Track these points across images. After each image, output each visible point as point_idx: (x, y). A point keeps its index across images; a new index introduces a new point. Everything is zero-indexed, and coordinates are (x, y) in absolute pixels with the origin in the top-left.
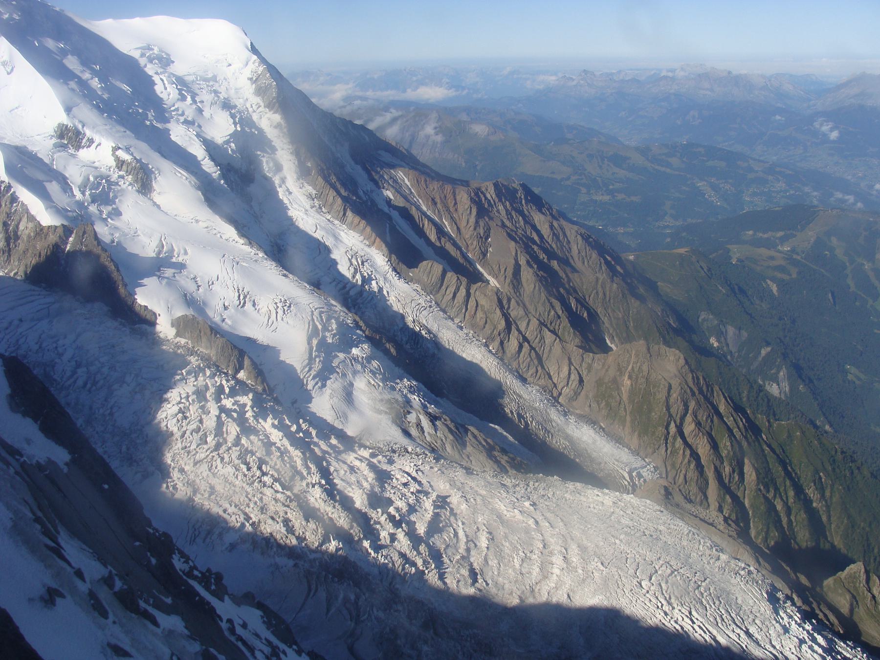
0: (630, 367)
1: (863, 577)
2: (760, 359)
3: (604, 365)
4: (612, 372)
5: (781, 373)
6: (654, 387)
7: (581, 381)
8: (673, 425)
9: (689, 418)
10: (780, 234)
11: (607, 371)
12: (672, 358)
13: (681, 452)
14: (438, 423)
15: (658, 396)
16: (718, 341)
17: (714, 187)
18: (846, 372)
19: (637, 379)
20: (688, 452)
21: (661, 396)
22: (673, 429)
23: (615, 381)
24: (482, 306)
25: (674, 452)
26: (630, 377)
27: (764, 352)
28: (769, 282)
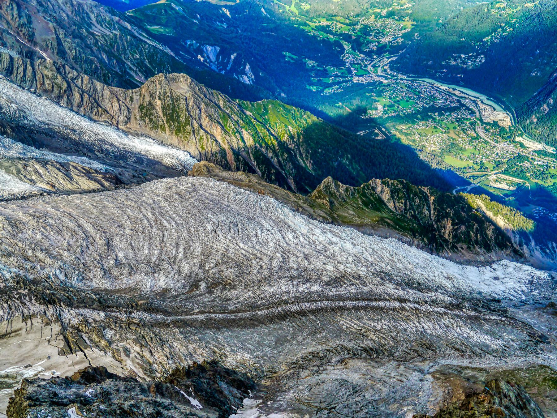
0: (158, 93)
1: (333, 185)
2: (231, 62)
3: (140, 96)
4: (147, 99)
6: (177, 101)
7: (128, 109)
8: (195, 122)
9: (204, 115)
11: (144, 98)
12: (182, 80)
13: (205, 138)
14: (49, 167)
16: (203, 57)
18: (285, 56)
19: (164, 99)
20: (209, 137)
22: (196, 125)
23: (150, 104)
24: (47, 76)
25: (201, 139)
26: (160, 99)
27: (233, 57)
28: (224, 9)
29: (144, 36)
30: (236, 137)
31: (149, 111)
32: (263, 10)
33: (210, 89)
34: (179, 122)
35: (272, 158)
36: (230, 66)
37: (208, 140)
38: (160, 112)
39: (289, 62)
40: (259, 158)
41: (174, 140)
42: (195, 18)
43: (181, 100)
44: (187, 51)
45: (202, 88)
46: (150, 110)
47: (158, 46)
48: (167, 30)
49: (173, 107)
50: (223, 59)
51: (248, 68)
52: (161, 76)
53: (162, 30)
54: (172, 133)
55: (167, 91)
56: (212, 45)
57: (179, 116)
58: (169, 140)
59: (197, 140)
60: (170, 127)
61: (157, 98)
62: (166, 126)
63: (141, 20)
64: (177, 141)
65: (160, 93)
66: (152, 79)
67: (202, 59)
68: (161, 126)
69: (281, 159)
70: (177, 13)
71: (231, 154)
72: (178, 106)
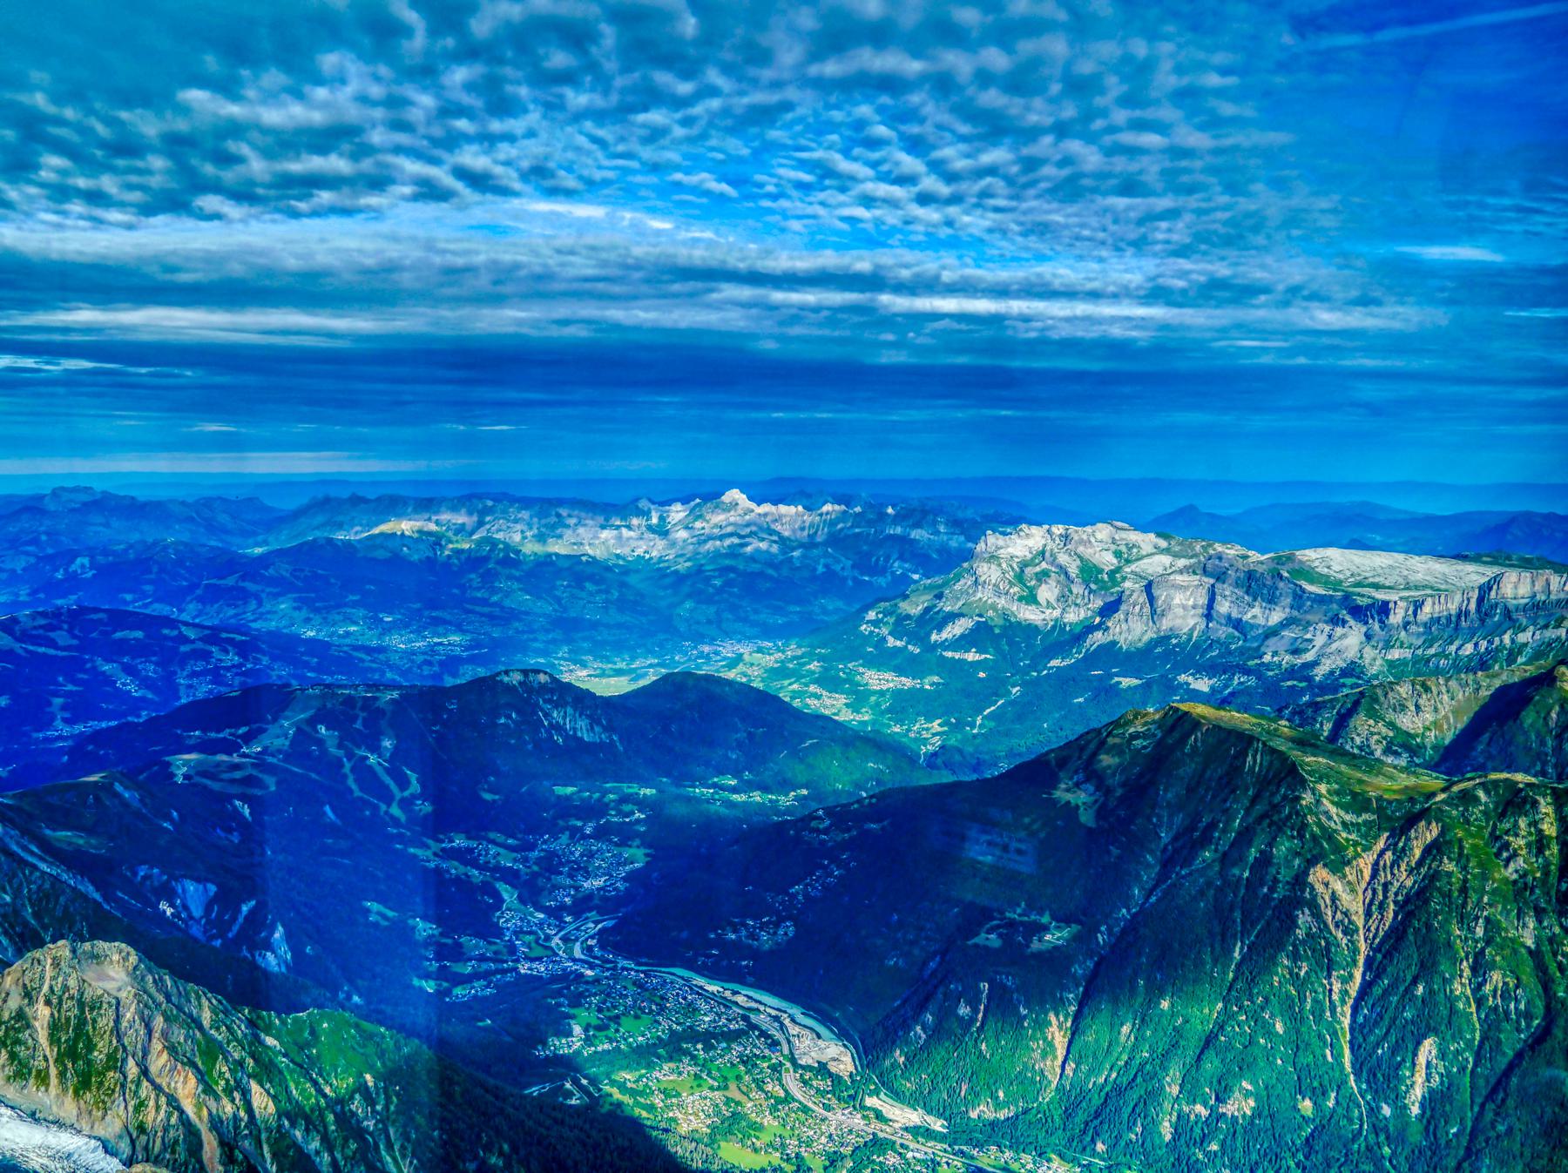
0: (46, 988)
2: (241, 919)
5: (277, 935)
6: (92, 1009)
8: (131, 1062)
9: (157, 1045)
10: (241, 731)
12: (116, 957)
13: (152, 1103)
15: (101, 1023)
16: (172, 905)
17: (129, 670)
18: (368, 911)
19: (60, 1003)
20: (163, 1100)
21: (105, 1022)
22: (132, 1069)
23: (20, 1015)
26: (48, 1003)
27: (245, 909)
28: (237, 803)
29: (32, 853)
30: (233, 1101)
31: (12, 1033)
32: (327, 809)
33: (180, 983)
34: (89, 1063)
35: (317, 1153)
36: (236, 928)
37: (158, 1108)
38: (43, 1037)
39: (376, 925)
40: (285, 1156)
41: (69, 1108)
42: (169, 818)
43: (105, 1006)
44: (136, 891)
45: (161, 979)
46: (18, 1031)
47: (65, 876)
48: (93, 841)
49: (82, 1022)
50: (221, 914)
51: (279, 934)
52: (62, 948)
53: (81, 842)
54: (65, 1090)
55: (72, 983)
56: (198, 880)
57: (90, 1047)
58: (55, 1109)
59: (130, 1109)
60: (62, 1075)
61: (42, 1000)
62: (53, 1071)
63: (31, 816)
64: (75, 1112)
65: (51, 988)
66: (38, 954)
67: (169, 911)
68: (39, 1072)
69: (338, 1156)
70: (125, 804)
71: (215, 1144)
72: (94, 1021)
